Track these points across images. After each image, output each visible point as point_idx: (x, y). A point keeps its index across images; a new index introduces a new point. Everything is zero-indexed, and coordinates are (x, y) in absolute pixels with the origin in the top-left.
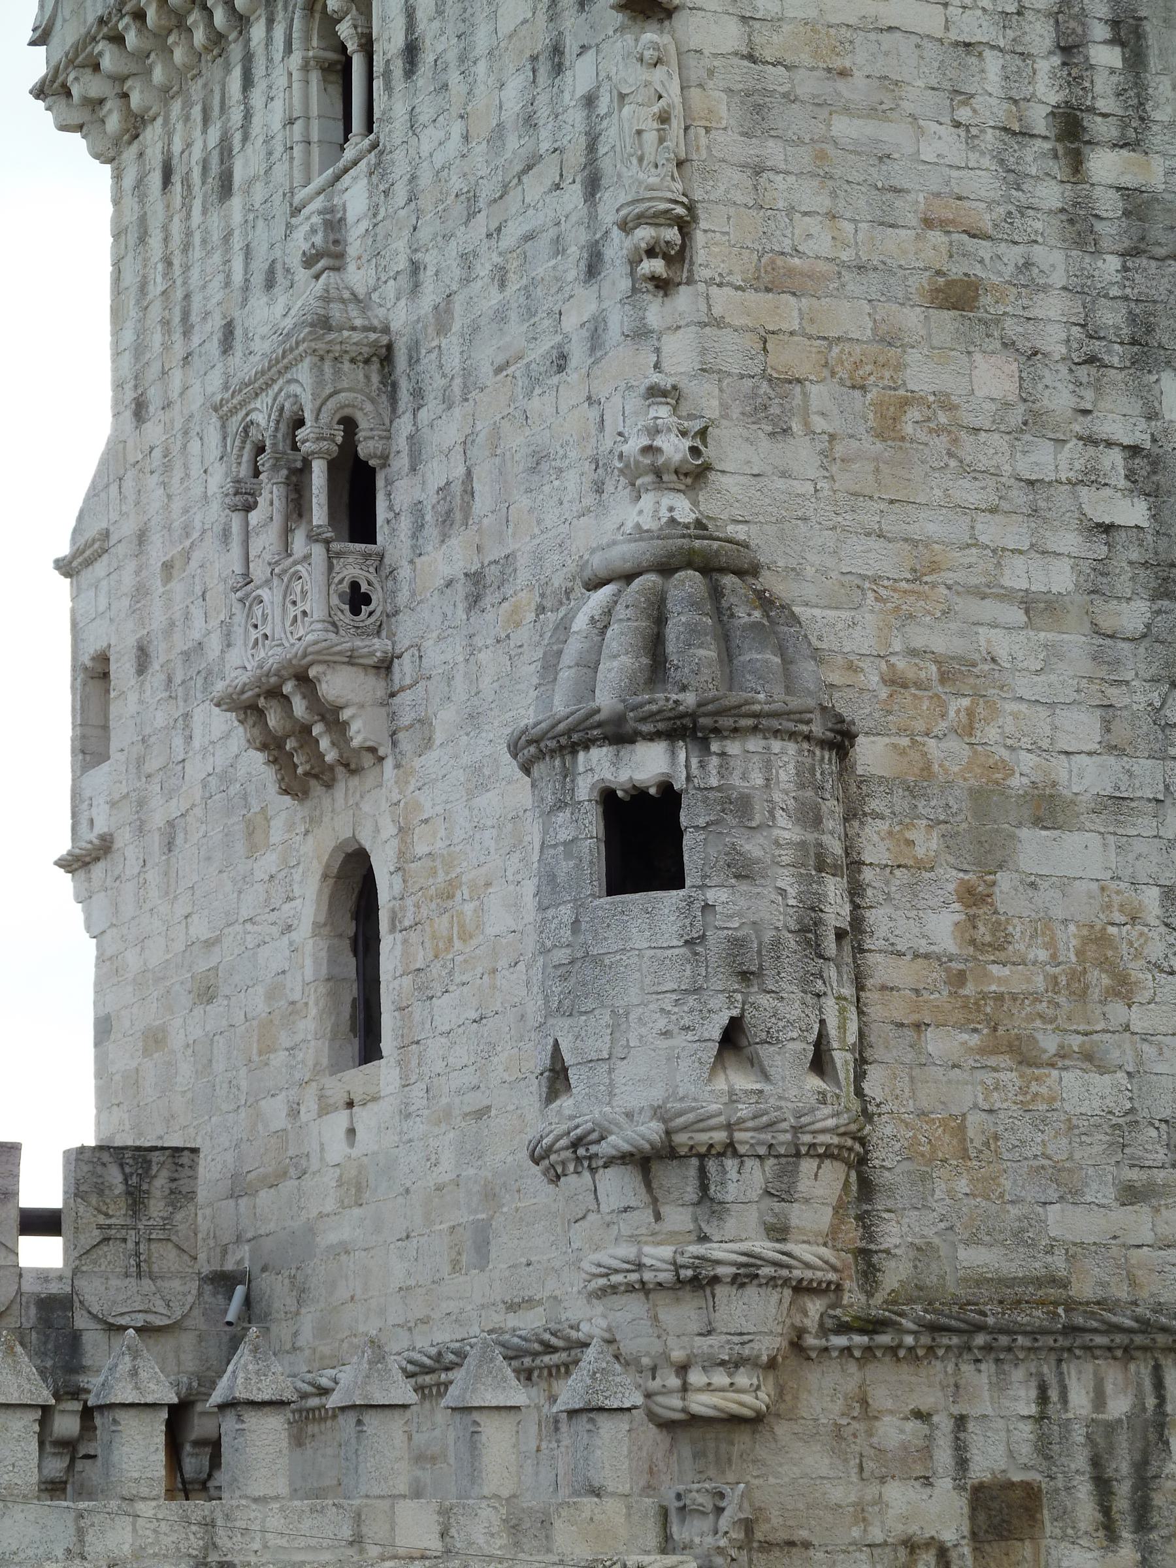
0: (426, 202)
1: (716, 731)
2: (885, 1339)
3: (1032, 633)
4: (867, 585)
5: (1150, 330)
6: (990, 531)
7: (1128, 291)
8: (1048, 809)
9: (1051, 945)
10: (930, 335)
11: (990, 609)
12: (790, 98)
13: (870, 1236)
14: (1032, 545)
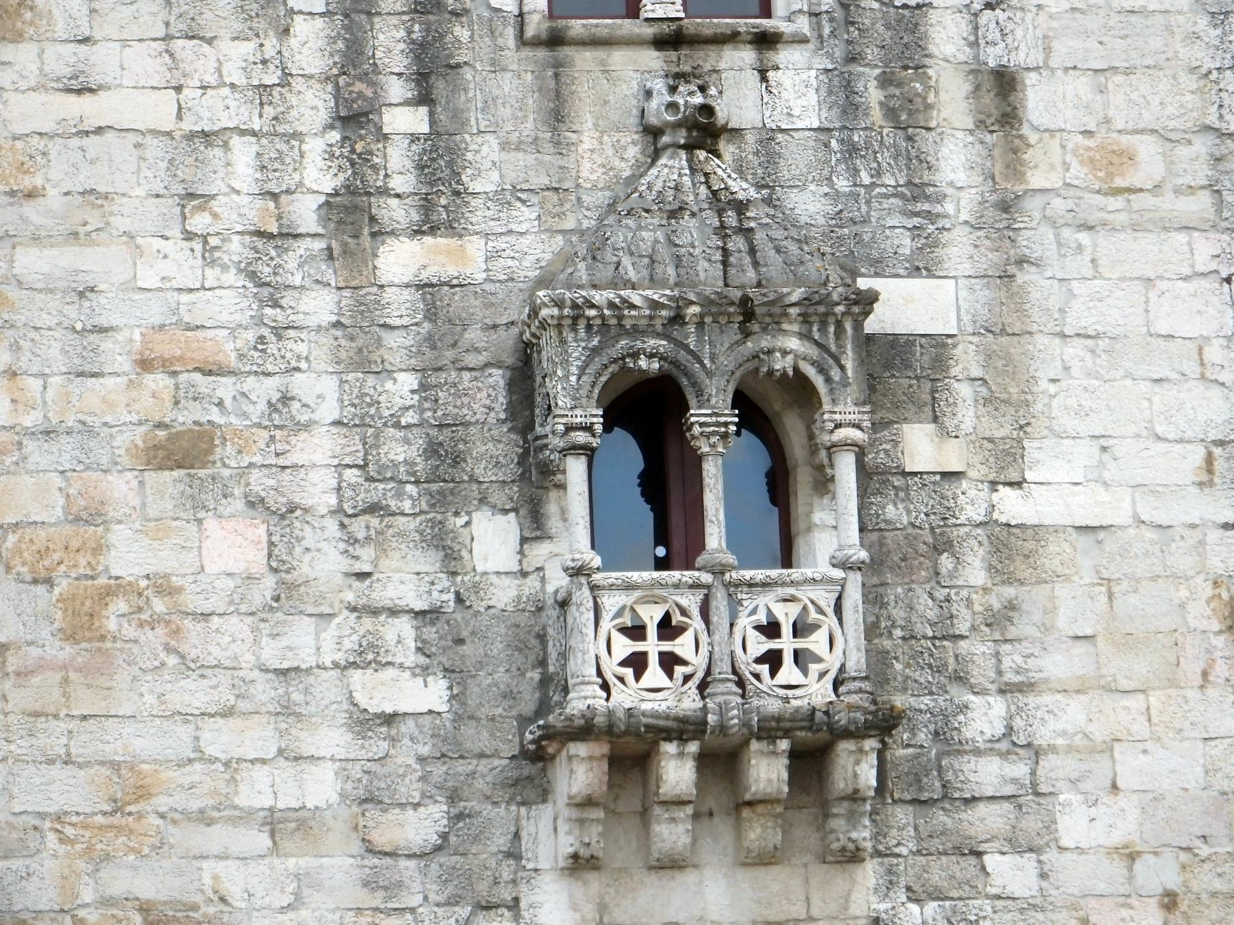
3: (276, 861)
4: (48, 824)
5: (457, 460)
6: (220, 739)
10: (144, 504)
11: (217, 837)
14: (281, 752)
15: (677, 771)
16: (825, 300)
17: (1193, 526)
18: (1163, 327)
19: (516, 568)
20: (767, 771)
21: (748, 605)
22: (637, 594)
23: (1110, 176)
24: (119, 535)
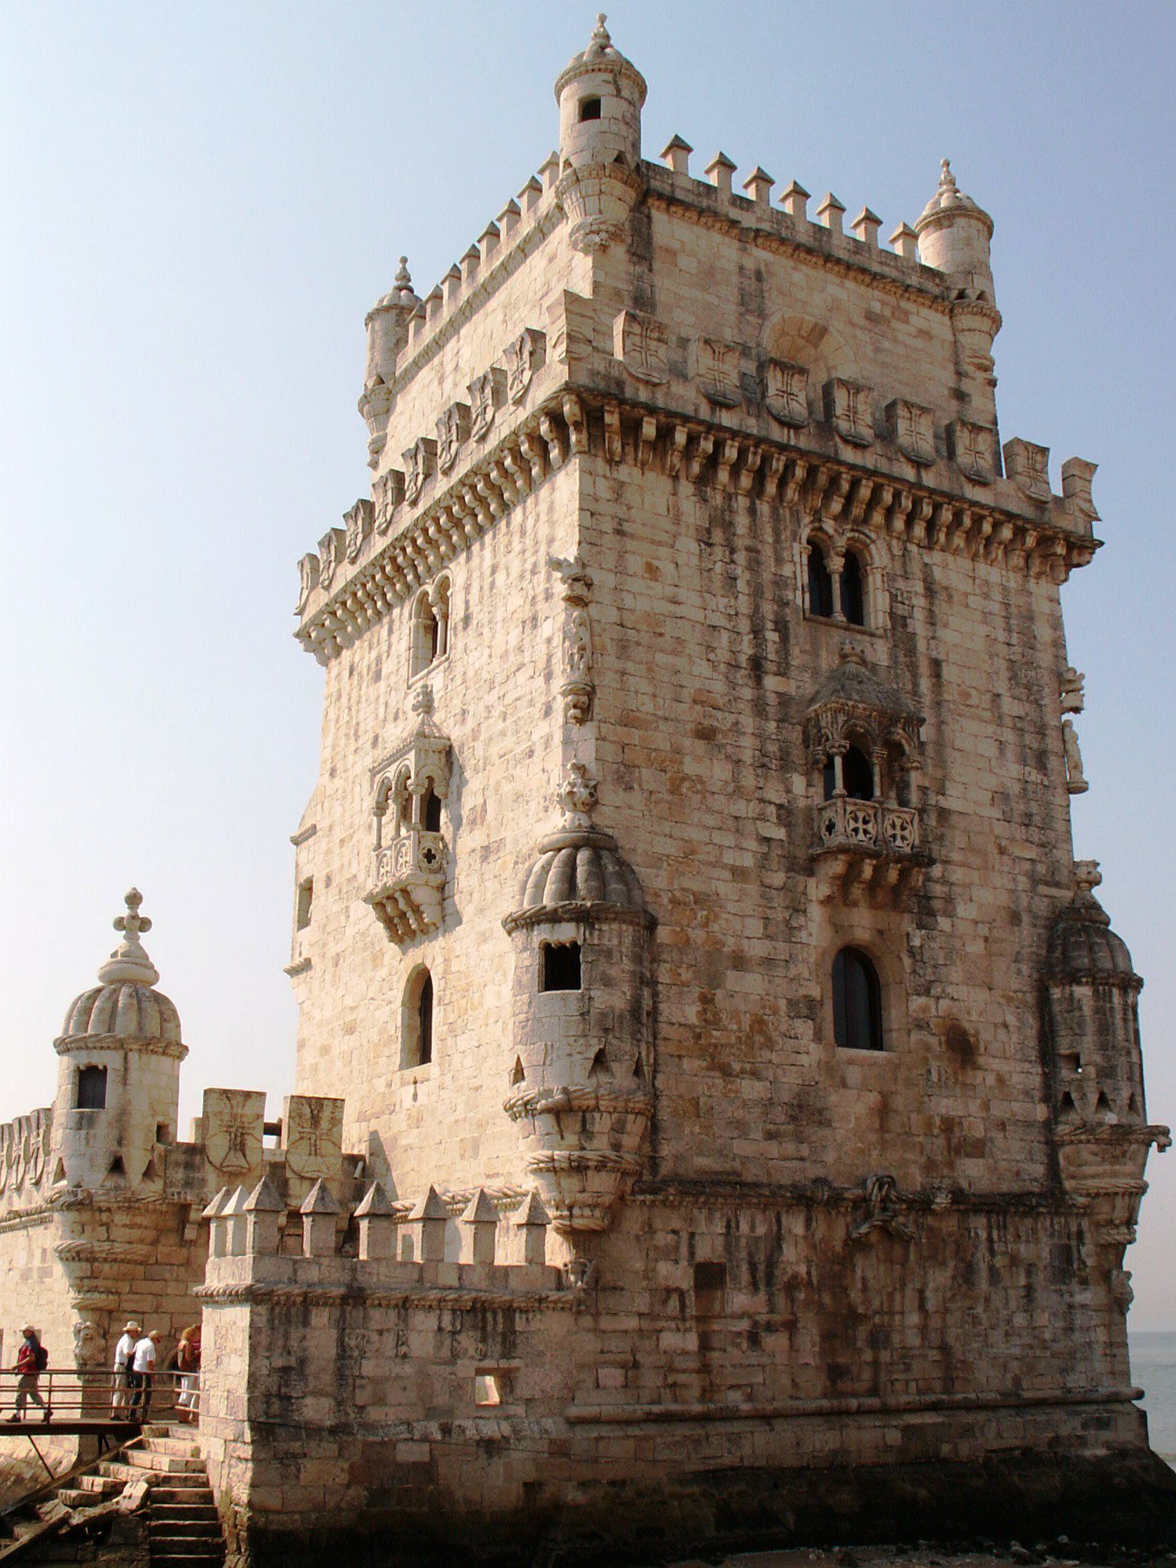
0: (470, 683)
1: (598, 919)
2: (661, 1197)
5: (788, 754)
6: (717, 838)
8: (739, 962)
9: (739, 1022)
11: (717, 872)
12: (638, 644)
13: (655, 1150)
15: (868, 871)
24: (687, 759)
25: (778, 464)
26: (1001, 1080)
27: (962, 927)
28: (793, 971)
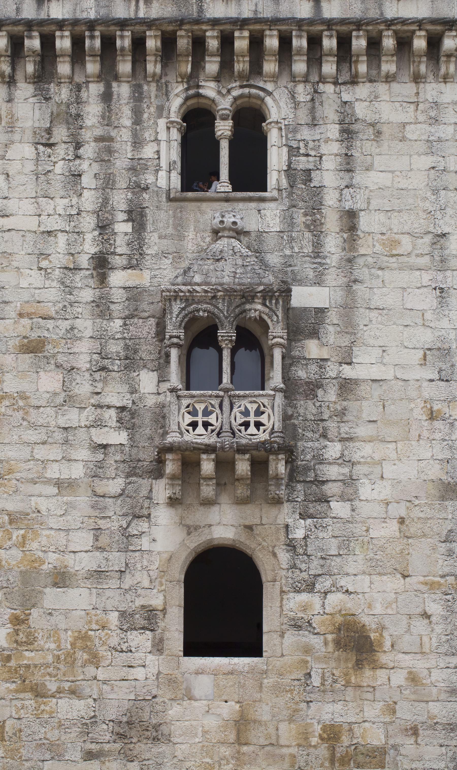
3: (59, 498)
5: (136, 351)
6: (41, 453)
7: (126, 335)
14: (63, 458)
15: (208, 466)
16: (271, 291)
17: (418, 380)
18: (409, 306)
19: (156, 392)
20: (243, 467)
21: (237, 404)
22: (195, 399)
23: (391, 250)
25: (124, 41)
26: (413, 678)
27: (365, 510)
28: (128, 581)
